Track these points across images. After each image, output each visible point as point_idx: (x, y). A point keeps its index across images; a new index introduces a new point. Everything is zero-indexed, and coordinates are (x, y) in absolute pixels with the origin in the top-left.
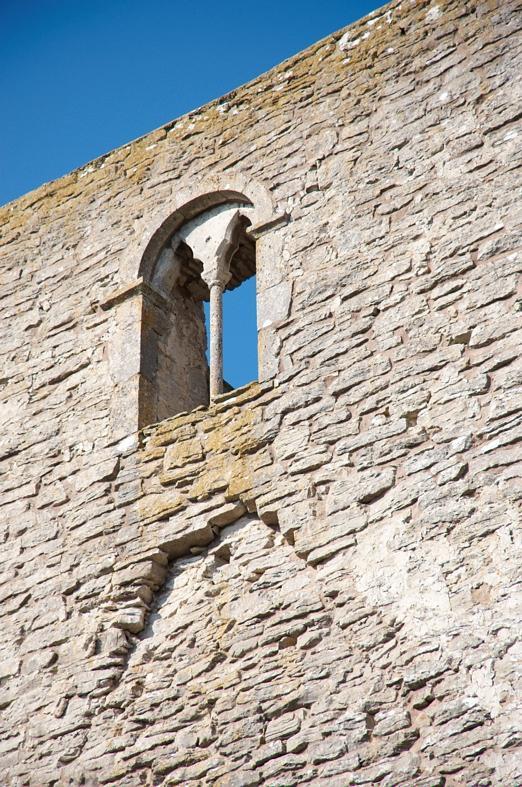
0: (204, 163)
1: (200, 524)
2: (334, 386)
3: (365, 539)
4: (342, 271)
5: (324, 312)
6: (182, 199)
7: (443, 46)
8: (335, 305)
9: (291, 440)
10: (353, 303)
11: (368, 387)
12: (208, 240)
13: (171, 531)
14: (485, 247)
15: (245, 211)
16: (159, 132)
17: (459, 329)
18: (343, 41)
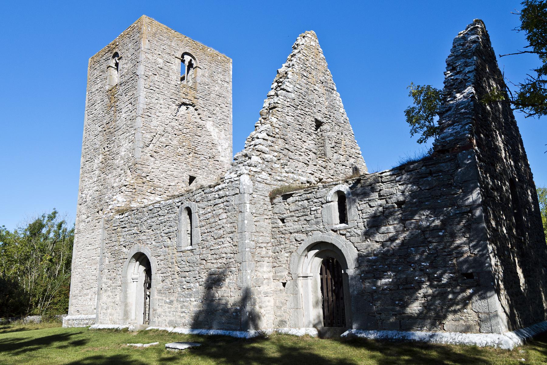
0: (190, 48)
1: (188, 103)
2: (206, 98)
3: (208, 122)
4: (207, 83)
5: (205, 87)
6: (187, 51)
7: (220, 63)
8: (206, 87)
9: (200, 101)
10: (209, 89)
11: (209, 102)
12: (187, 58)
13: (184, 100)
14: (223, 96)
15: (193, 59)
16: (184, 36)
17: (219, 103)
18: (209, 49)
